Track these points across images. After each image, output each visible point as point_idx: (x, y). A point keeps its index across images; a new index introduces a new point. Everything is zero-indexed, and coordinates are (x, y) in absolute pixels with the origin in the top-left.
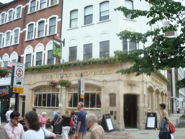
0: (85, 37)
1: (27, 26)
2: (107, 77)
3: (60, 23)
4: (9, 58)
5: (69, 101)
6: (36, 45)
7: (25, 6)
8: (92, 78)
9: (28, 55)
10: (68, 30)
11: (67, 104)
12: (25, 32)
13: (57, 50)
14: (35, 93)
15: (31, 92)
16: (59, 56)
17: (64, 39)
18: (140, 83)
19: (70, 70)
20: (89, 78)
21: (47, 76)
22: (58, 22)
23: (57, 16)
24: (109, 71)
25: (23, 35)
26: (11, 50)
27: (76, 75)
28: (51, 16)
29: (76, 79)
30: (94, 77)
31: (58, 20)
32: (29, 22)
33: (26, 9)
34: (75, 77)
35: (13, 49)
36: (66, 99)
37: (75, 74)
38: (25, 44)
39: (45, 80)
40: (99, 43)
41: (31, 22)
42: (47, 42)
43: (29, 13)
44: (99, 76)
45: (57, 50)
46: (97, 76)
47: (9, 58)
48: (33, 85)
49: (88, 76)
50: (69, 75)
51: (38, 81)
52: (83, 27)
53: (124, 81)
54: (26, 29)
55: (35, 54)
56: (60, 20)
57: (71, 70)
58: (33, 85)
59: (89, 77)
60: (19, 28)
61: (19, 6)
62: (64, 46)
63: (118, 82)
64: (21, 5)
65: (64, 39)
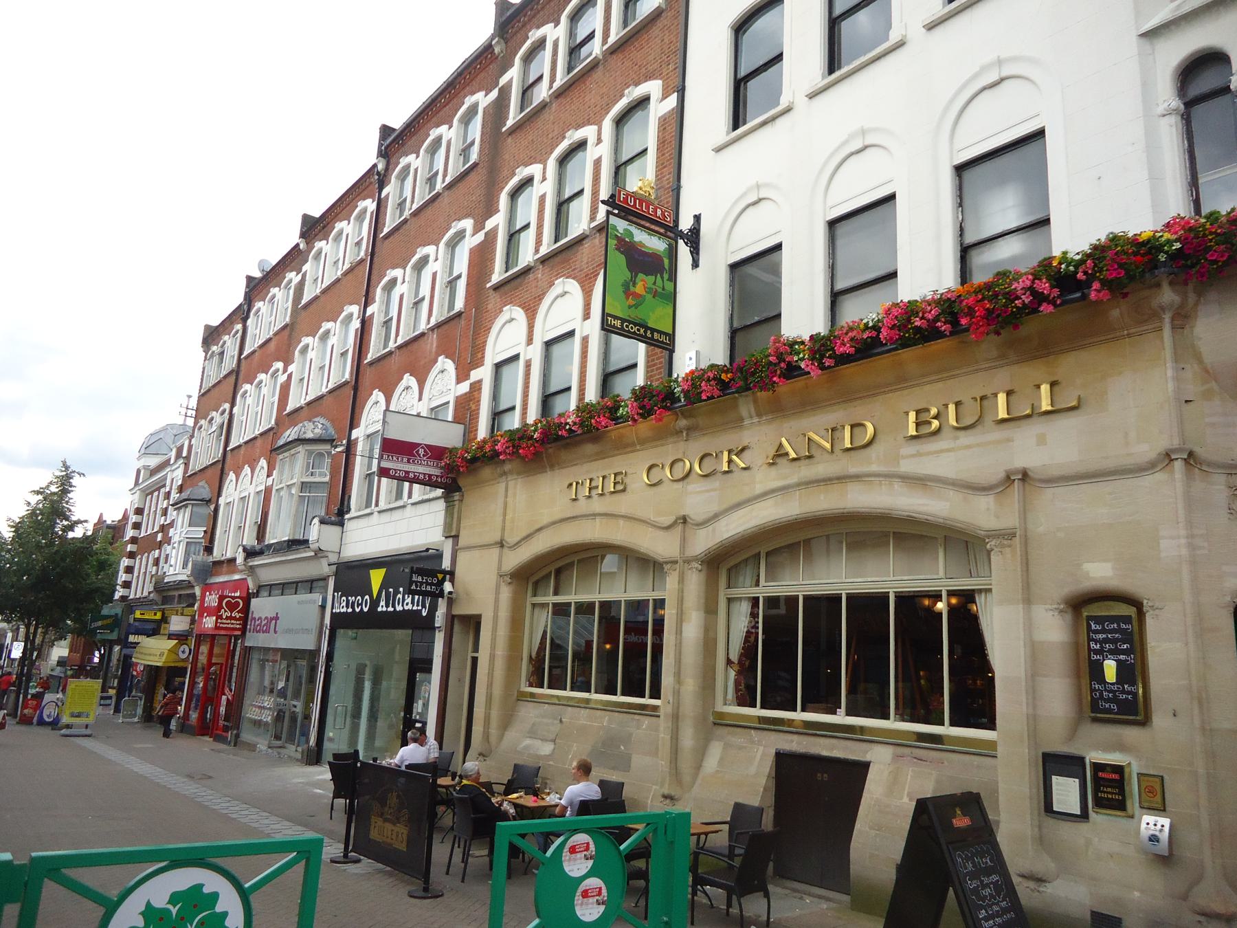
1: (503, 199)
2: (1041, 440)
3: (674, 126)
4: (420, 399)
6: (540, 298)
7: (494, 94)
8: (906, 467)
10: (718, 150)
11: (726, 679)
12: (491, 237)
13: (639, 288)
14: (540, 599)
16: (653, 330)
17: (697, 218)
19: (738, 423)
20: (874, 468)
21: (594, 484)
22: (663, 122)
24: (1053, 384)
25: (481, 258)
26: (431, 352)
27: (780, 454)
28: (622, 96)
34: (773, 471)
35: (438, 347)
36: (708, 645)
37: (772, 452)
38: (494, 298)
39: (583, 506)
41: (523, 173)
44: (965, 439)
45: (639, 288)
47: (420, 399)
48: (518, 544)
50: (730, 461)
51: (545, 521)
54: (498, 221)
55: (535, 353)
57: (742, 419)
58: (518, 544)
59: (872, 462)
60: (467, 224)
61: (469, 101)
62: (695, 264)
63: (1160, 476)
64: (479, 96)
65: (697, 218)
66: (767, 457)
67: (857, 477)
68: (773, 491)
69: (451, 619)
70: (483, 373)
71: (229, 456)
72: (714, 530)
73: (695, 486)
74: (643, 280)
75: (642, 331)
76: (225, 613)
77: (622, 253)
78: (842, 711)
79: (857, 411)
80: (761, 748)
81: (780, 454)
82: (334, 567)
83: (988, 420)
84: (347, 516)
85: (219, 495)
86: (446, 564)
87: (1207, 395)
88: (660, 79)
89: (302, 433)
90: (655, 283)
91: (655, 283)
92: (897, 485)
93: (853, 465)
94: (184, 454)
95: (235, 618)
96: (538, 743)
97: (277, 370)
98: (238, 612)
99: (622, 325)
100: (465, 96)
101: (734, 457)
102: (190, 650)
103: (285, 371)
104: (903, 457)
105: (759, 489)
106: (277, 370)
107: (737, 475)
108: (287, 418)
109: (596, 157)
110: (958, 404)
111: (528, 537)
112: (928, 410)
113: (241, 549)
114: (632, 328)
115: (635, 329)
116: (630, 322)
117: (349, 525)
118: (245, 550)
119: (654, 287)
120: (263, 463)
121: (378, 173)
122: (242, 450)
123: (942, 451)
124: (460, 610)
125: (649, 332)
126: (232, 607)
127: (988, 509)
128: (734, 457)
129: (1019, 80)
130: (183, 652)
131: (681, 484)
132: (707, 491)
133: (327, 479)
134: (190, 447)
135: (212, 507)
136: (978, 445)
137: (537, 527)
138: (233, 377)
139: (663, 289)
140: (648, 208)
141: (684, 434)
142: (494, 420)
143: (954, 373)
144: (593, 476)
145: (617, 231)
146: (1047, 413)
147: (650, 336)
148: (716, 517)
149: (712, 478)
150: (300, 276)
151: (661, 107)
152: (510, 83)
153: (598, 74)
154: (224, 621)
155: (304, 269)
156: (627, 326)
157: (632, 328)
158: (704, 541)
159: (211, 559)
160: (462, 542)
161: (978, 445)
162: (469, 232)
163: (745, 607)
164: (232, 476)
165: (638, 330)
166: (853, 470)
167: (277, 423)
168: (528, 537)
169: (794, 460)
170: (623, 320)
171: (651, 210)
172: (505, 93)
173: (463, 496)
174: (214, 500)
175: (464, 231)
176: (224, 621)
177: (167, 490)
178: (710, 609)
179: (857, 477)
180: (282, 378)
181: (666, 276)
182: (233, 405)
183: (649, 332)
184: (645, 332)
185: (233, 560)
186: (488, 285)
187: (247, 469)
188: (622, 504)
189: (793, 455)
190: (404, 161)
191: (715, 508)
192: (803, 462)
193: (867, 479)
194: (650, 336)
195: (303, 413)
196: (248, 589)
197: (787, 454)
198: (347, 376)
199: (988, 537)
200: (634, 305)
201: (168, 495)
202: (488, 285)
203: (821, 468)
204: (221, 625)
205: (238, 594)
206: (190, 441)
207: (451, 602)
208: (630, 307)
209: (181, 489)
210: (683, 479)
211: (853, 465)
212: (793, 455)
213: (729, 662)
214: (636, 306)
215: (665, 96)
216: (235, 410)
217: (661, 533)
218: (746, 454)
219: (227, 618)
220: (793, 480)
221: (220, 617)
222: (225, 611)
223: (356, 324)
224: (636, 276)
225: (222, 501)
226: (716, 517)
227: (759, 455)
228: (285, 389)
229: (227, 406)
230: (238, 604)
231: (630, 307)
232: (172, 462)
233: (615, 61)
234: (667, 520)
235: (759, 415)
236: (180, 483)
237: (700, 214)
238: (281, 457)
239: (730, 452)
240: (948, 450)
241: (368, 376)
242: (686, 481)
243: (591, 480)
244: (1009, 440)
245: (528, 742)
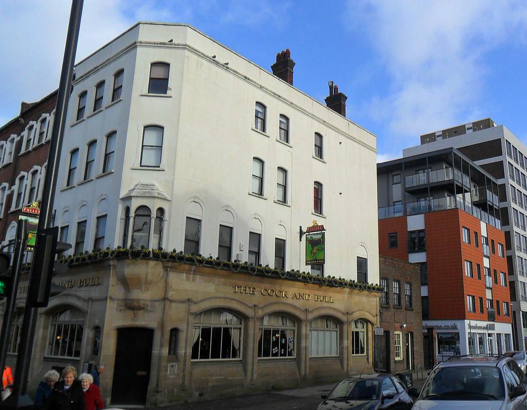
0: (100, 199)
7: (19, 138)
17: (55, 211)
18: (157, 304)
20: (73, 293)
32: (32, 168)
33: (19, 144)
36: (44, 338)
38: (10, 216)
40: (96, 218)
43: (23, 151)
44: (87, 288)
46: (83, 289)
52: (64, 192)
53: (118, 300)
54: (15, 188)
59: (72, 292)
78: (66, 355)
87: (118, 284)
140: (35, 211)
153: (43, 148)
163: (53, 327)
166: (71, 293)
172: (22, 138)
175: (5, 187)
178: (45, 328)
186: (9, 212)
202: (9, 212)
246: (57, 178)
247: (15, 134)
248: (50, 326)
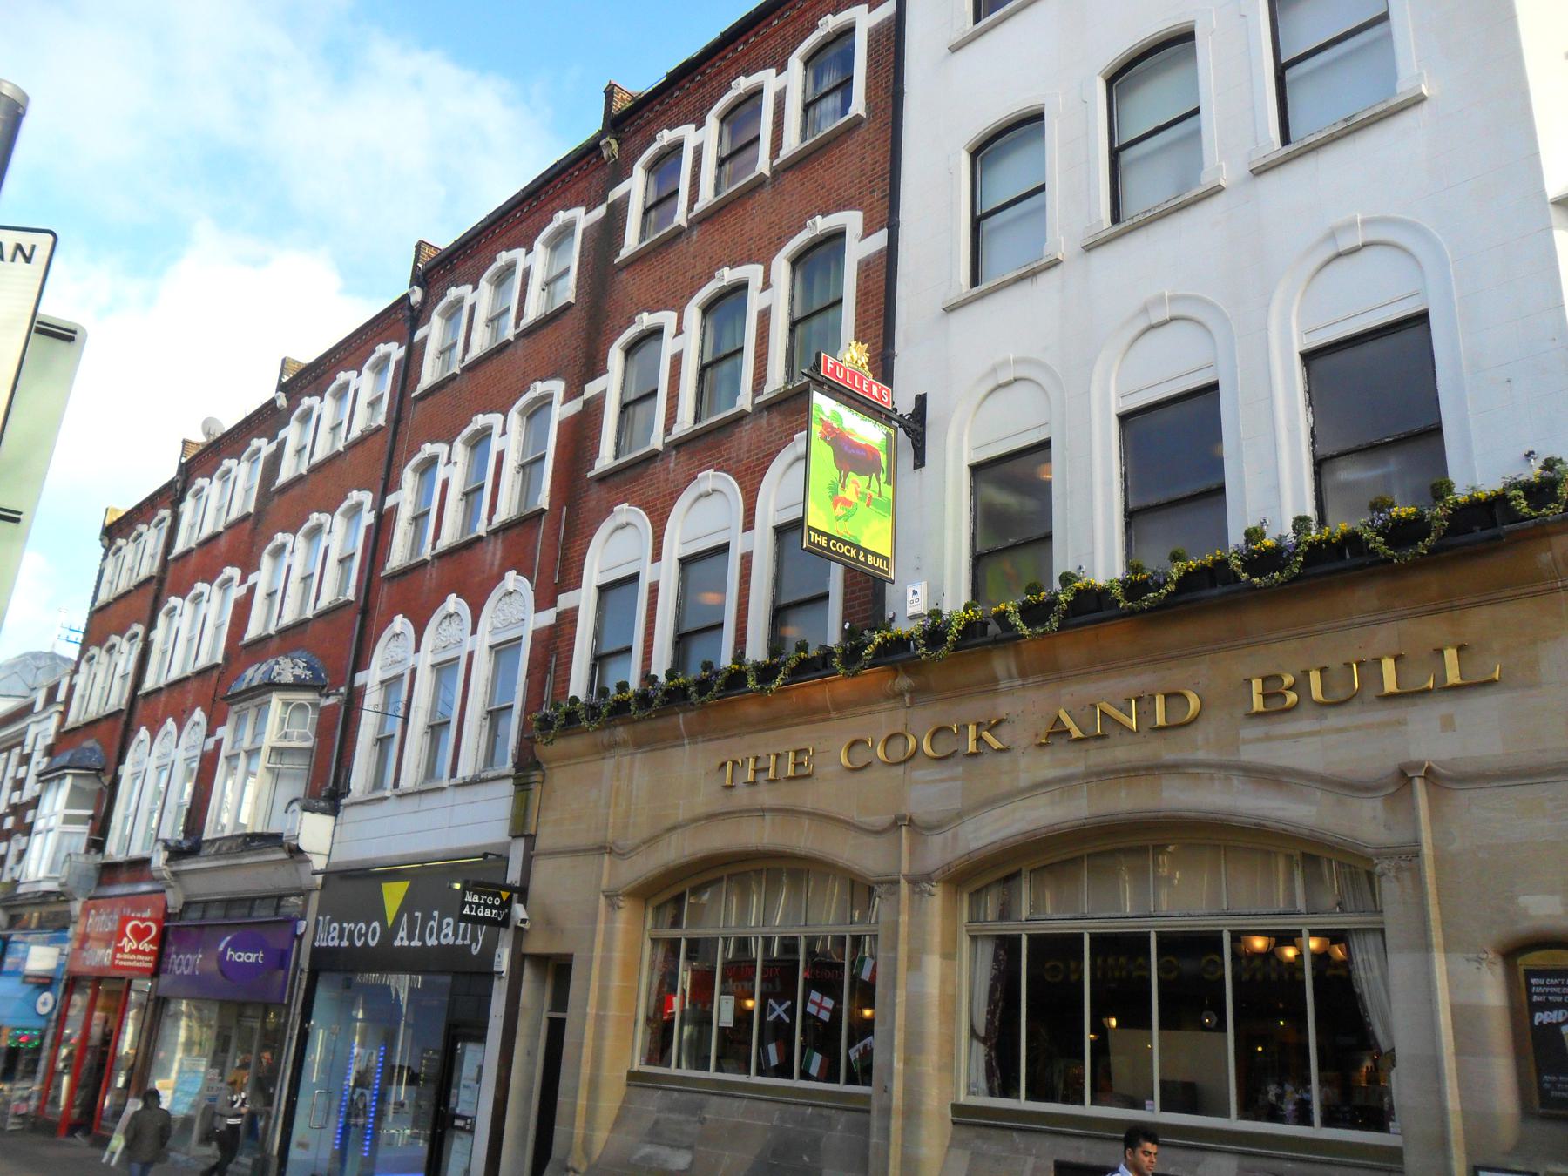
1: (615, 357)
2: (1448, 724)
3: (883, 271)
5: (982, 1032)
7: (600, 212)
8: (1251, 754)
9: (616, 589)
12: (594, 409)
15: (624, 917)
16: (867, 552)
17: (921, 400)
19: (989, 686)
20: (1201, 755)
21: (761, 765)
22: (865, 266)
23: (851, 220)
24: (1461, 649)
25: (579, 435)
26: (492, 565)
28: (802, 227)
29: (1051, 773)
30: (1268, 738)
31: (859, 248)
34: (1046, 757)
35: (504, 559)
37: (1044, 728)
38: (596, 492)
39: (742, 797)
41: (646, 320)
42: (771, 456)
44: (1334, 719)
45: (849, 493)
46: (1305, 724)
49: (1198, 734)
50: (979, 739)
51: (682, 815)
54: (611, 384)
55: (667, 575)
56: (880, 240)
57: (995, 680)
59: (1200, 746)
60: (557, 387)
61: (561, 217)
65: (921, 400)
66: (1037, 735)
67: (1174, 768)
68: (1047, 783)
69: (519, 959)
70: (584, 599)
71: (140, 704)
72: (955, 837)
73: (922, 774)
74: (854, 482)
75: (853, 552)
76: (129, 944)
77: (829, 443)
79: (1175, 676)
80: (1031, 1161)
81: (1058, 732)
82: (319, 878)
83: (1371, 694)
84: (344, 801)
85: (121, 759)
86: (514, 876)
88: (861, 209)
89: (274, 673)
90: (869, 486)
91: (869, 486)
92: (1237, 781)
93: (1168, 751)
94: (61, 696)
95: (143, 953)
96: (665, 1152)
97: (231, 579)
98: (150, 942)
99: (828, 544)
100: (555, 211)
101: (986, 735)
102: (56, 1001)
103: (243, 580)
104: (1245, 742)
105: (1025, 779)
106: (231, 579)
107: (987, 761)
108: (241, 651)
109: (764, 305)
110: (1323, 670)
111: (652, 840)
112: (1279, 678)
113: (160, 846)
114: (840, 548)
115: (844, 549)
116: (838, 540)
117: (347, 815)
118: (167, 846)
119: (868, 491)
120: (199, 715)
121: (411, 307)
122: (163, 697)
123: (1301, 735)
124: (535, 946)
125: (862, 554)
126: (140, 934)
127: (1375, 818)
128: (986, 735)
129: (1379, 247)
130: (45, 1004)
131: (900, 770)
132: (942, 781)
133: (308, 744)
134: (71, 688)
135: (106, 780)
136: (1358, 728)
137: (668, 823)
138: (153, 586)
139: (880, 495)
141: (907, 700)
142: (594, 666)
143: (1317, 628)
144: (761, 753)
145: (822, 413)
146: (1455, 687)
147: (863, 559)
148: (960, 815)
149: (951, 761)
150: (274, 445)
151: (859, 248)
152: (626, 198)
154: (126, 956)
155: (281, 435)
156: (834, 545)
157: (840, 548)
158: (939, 852)
159: (99, 859)
160: (542, 843)
161: (1358, 728)
162: (559, 395)
164: (143, 733)
165: (849, 551)
167: (226, 657)
168: (652, 840)
169: (1079, 740)
170: (830, 537)
171: (865, 386)
173: (544, 776)
174: (113, 767)
176: (126, 956)
177: (27, 750)
179: (1174, 768)
180: (237, 592)
181: (883, 477)
182: (151, 626)
183: (862, 554)
184: (857, 554)
185: (146, 862)
187: (170, 724)
188: (809, 797)
189: (1076, 733)
190: (453, 293)
191: (957, 804)
192: (1093, 745)
193: (1191, 771)
194: (863, 559)
195: (274, 644)
196: (166, 906)
197: (1068, 732)
198: (350, 594)
199: (1378, 856)
200: (843, 516)
201: (25, 760)
202: (590, 475)
203: (1121, 753)
204: (122, 963)
205: (147, 914)
206: (71, 680)
207: (520, 933)
208: (838, 519)
209: (50, 751)
210: (905, 762)
211: (1168, 751)
212: (1076, 733)
213: (973, 1033)
214: (846, 517)
215: (868, 232)
216: (158, 635)
217: (871, 839)
218: (1004, 730)
219: (132, 952)
220: (1078, 767)
221: (121, 950)
222: (130, 941)
223: (368, 518)
224: (846, 476)
225: (126, 770)
226: (960, 815)
227: (1020, 734)
228: (242, 610)
229: (139, 629)
230: (149, 929)
231: (838, 519)
232: (38, 707)
233: (791, 181)
234: (882, 819)
235: (1023, 674)
236: (50, 741)
237: (925, 394)
238: (236, 708)
239: (978, 725)
240: (1312, 734)
241: (384, 595)
242: (909, 765)
243: (757, 759)
244: (1401, 723)
245: (647, 1150)
246: (1025, 194)
247: (576, 205)
248: (965, 943)
